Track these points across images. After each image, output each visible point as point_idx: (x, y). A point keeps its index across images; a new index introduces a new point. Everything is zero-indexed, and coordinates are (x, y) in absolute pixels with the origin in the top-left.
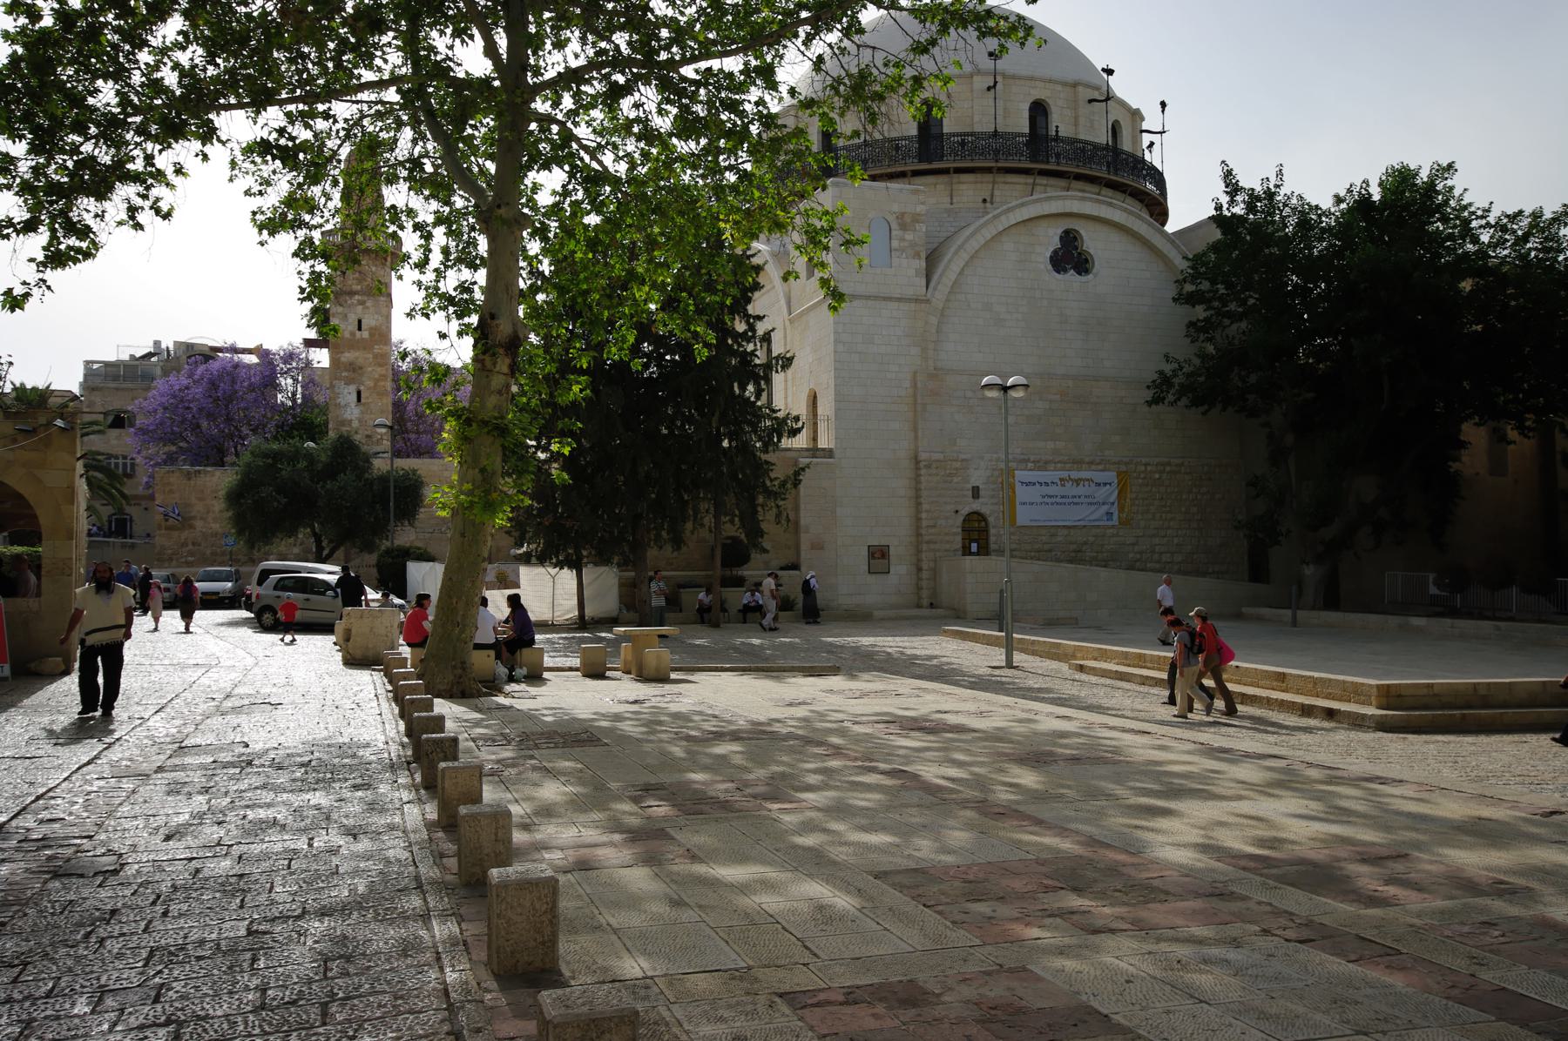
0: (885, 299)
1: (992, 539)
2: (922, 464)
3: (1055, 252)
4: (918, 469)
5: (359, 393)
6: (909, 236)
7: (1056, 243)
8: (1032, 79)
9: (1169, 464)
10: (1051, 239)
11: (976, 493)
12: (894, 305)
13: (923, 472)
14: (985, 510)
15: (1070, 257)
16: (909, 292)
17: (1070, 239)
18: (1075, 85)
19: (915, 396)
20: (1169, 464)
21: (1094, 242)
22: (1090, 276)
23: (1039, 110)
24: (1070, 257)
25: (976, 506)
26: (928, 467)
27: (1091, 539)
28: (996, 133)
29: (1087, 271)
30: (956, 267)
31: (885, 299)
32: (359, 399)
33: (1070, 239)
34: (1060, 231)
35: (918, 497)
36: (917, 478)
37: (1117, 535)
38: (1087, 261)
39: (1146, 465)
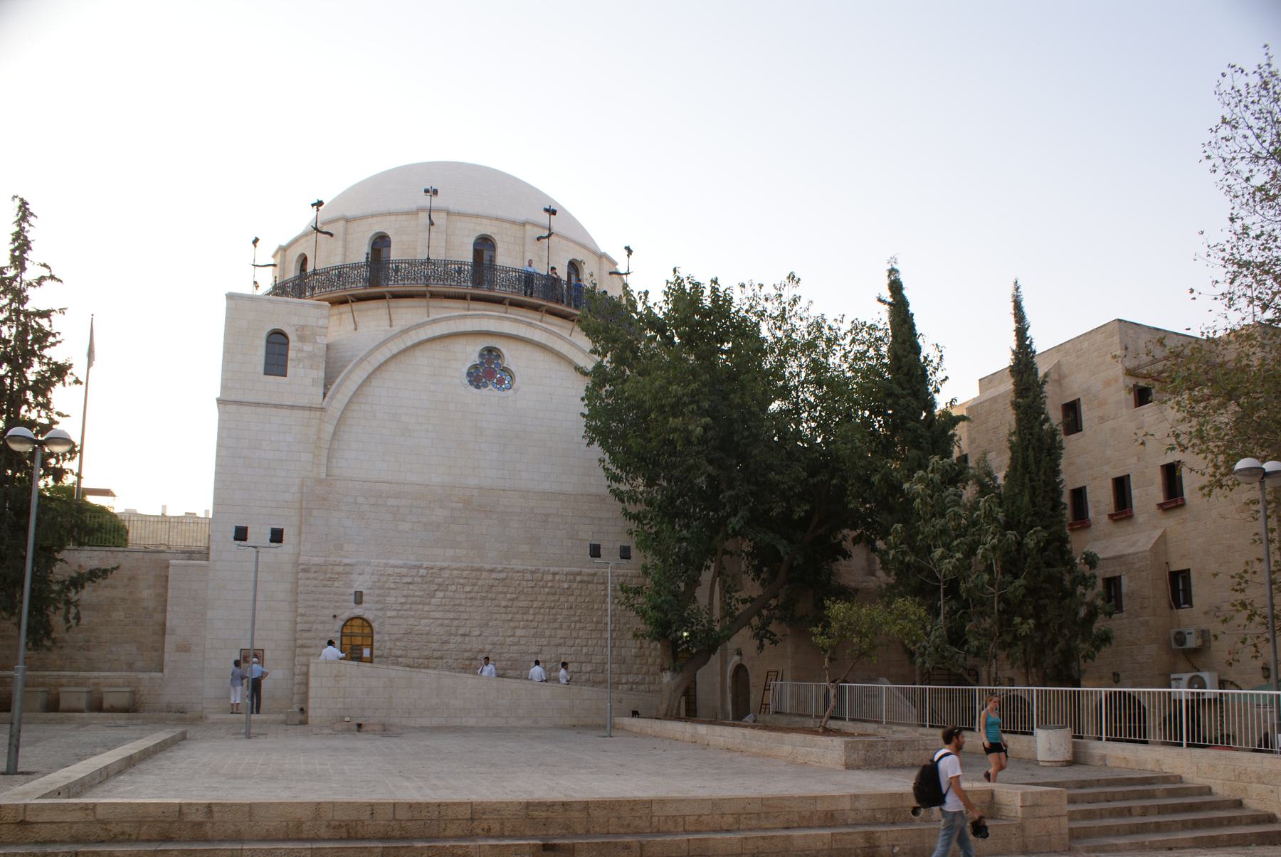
0: (275, 406)
3: (475, 367)
6: (308, 347)
7: (474, 358)
8: (477, 216)
9: (580, 574)
10: (470, 353)
11: (359, 598)
14: (368, 615)
15: (488, 370)
16: (304, 401)
17: (491, 354)
18: (523, 224)
21: (513, 357)
24: (488, 370)
25: (358, 611)
31: (275, 406)
33: (491, 354)
34: (479, 348)
37: (518, 643)
39: (554, 574)
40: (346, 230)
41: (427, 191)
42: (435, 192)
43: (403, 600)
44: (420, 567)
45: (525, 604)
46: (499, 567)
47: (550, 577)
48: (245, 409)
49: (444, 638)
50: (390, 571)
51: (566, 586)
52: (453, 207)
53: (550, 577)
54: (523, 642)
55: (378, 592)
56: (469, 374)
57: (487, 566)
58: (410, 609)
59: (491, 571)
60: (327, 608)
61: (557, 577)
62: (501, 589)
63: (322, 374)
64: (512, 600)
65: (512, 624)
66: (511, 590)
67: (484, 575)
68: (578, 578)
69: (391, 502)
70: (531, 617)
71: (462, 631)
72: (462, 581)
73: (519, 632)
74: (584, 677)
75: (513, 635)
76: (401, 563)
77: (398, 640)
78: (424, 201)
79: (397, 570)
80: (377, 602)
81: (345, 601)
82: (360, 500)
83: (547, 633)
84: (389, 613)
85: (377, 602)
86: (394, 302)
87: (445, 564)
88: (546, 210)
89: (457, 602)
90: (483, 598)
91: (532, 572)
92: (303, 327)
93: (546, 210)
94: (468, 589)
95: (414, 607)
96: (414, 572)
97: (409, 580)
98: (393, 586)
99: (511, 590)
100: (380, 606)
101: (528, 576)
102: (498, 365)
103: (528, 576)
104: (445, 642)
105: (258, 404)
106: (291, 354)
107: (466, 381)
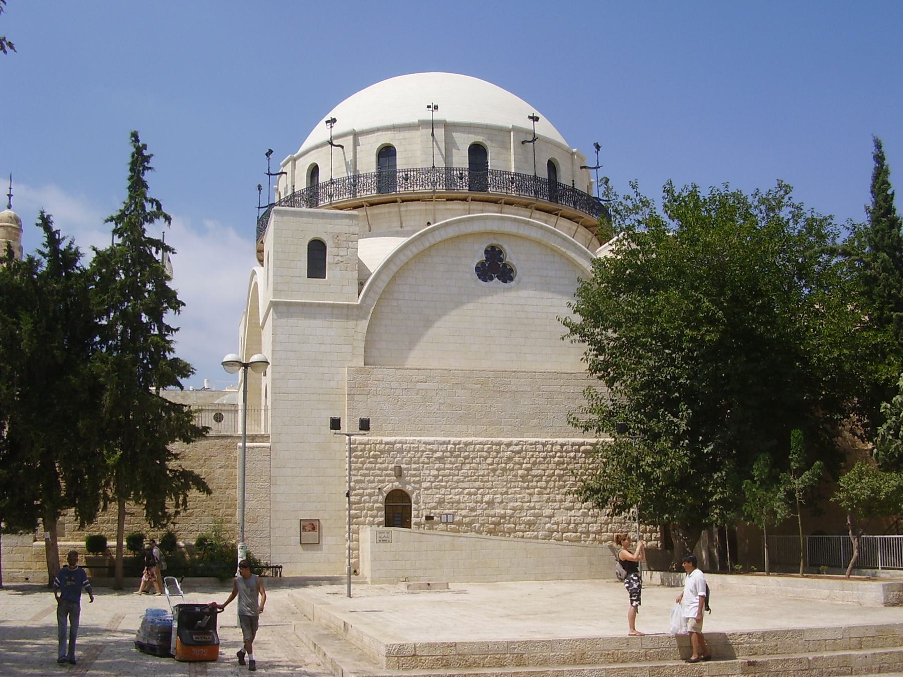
1: (414, 513)
6: (343, 252)
9: (583, 444)
11: (399, 473)
14: (409, 488)
22: (513, 283)
27: (509, 512)
29: (511, 279)
34: (484, 247)
38: (511, 270)
39: (562, 445)
41: (429, 107)
42: (436, 107)
43: (436, 473)
44: (449, 442)
46: (515, 440)
47: (558, 447)
49: (472, 505)
50: (422, 447)
51: (572, 454)
52: (450, 119)
53: (558, 447)
54: (538, 505)
55: (414, 466)
56: (477, 269)
58: (442, 481)
59: (509, 445)
60: (373, 482)
62: (516, 459)
63: (355, 274)
64: (528, 470)
65: (527, 491)
68: (582, 448)
70: (543, 484)
71: (486, 498)
72: (485, 454)
73: (535, 498)
74: (592, 536)
75: (530, 502)
76: (431, 439)
77: (435, 508)
78: (428, 115)
79: (429, 447)
80: (415, 476)
81: (387, 475)
82: (394, 385)
83: (558, 497)
84: (424, 485)
85: (415, 476)
86: (404, 207)
87: (470, 439)
88: (530, 117)
89: (481, 473)
90: (504, 470)
91: (544, 445)
93: (530, 117)
94: (489, 460)
98: (426, 460)
100: (418, 479)
102: (501, 260)
103: (540, 447)
104: (473, 510)
106: (328, 259)
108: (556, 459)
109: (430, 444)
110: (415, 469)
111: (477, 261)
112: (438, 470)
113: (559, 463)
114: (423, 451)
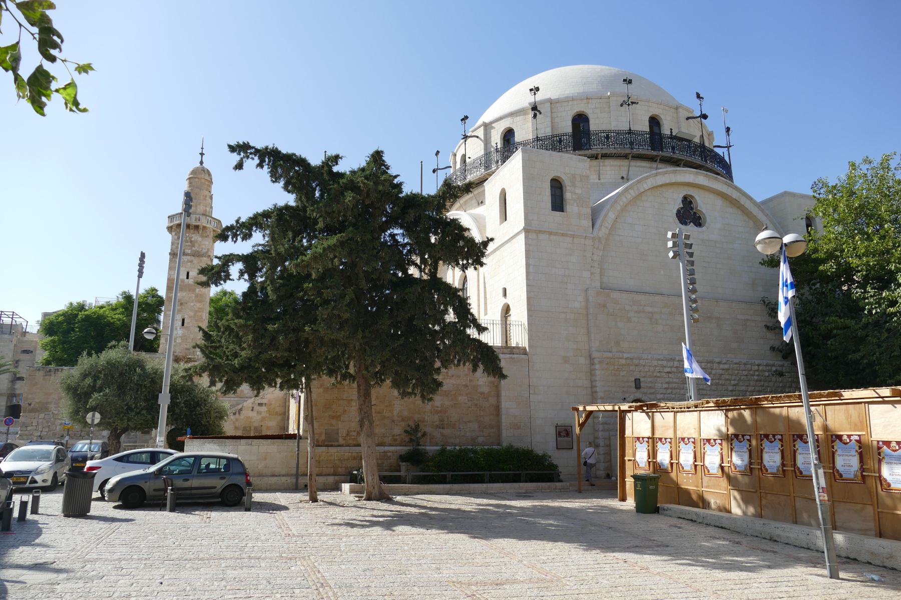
0: (563, 235)
2: (596, 361)
3: (678, 211)
4: (592, 364)
5: (183, 320)
7: (679, 204)
9: (773, 365)
12: (569, 240)
13: (597, 367)
15: (689, 214)
17: (687, 201)
18: (677, 108)
19: (587, 308)
20: (773, 365)
21: (704, 204)
22: (704, 228)
23: (654, 122)
24: (689, 214)
26: (600, 362)
28: (630, 132)
30: (612, 216)
32: (183, 324)
33: (687, 201)
34: (681, 196)
35: (593, 387)
36: (592, 372)
38: (700, 217)
39: (759, 365)
40: (551, 109)
43: (666, 386)
45: (744, 388)
46: (724, 361)
47: (756, 368)
48: (541, 236)
50: (655, 363)
53: (756, 368)
55: (649, 379)
57: (717, 360)
59: (719, 363)
61: (761, 368)
62: (727, 377)
66: (733, 377)
67: (715, 366)
69: (648, 309)
79: (660, 363)
82: (627, 308)
92: (574, 176)
95: (674, 391)
96: (671, 364)
97: (668, 370)
98: (658, 374)
99: (733, 377)
100: (652, 391)
101: (742, 367)
102: (692, 209)
105: (551, 233)
106: (568, 195)
107: (677, 221)
108: (756, 378)
109: (659, 360)
110: (650, 382)
111: (677, 208)
112: (668, 383)
113: (757, 381)
114: (655, 366)
